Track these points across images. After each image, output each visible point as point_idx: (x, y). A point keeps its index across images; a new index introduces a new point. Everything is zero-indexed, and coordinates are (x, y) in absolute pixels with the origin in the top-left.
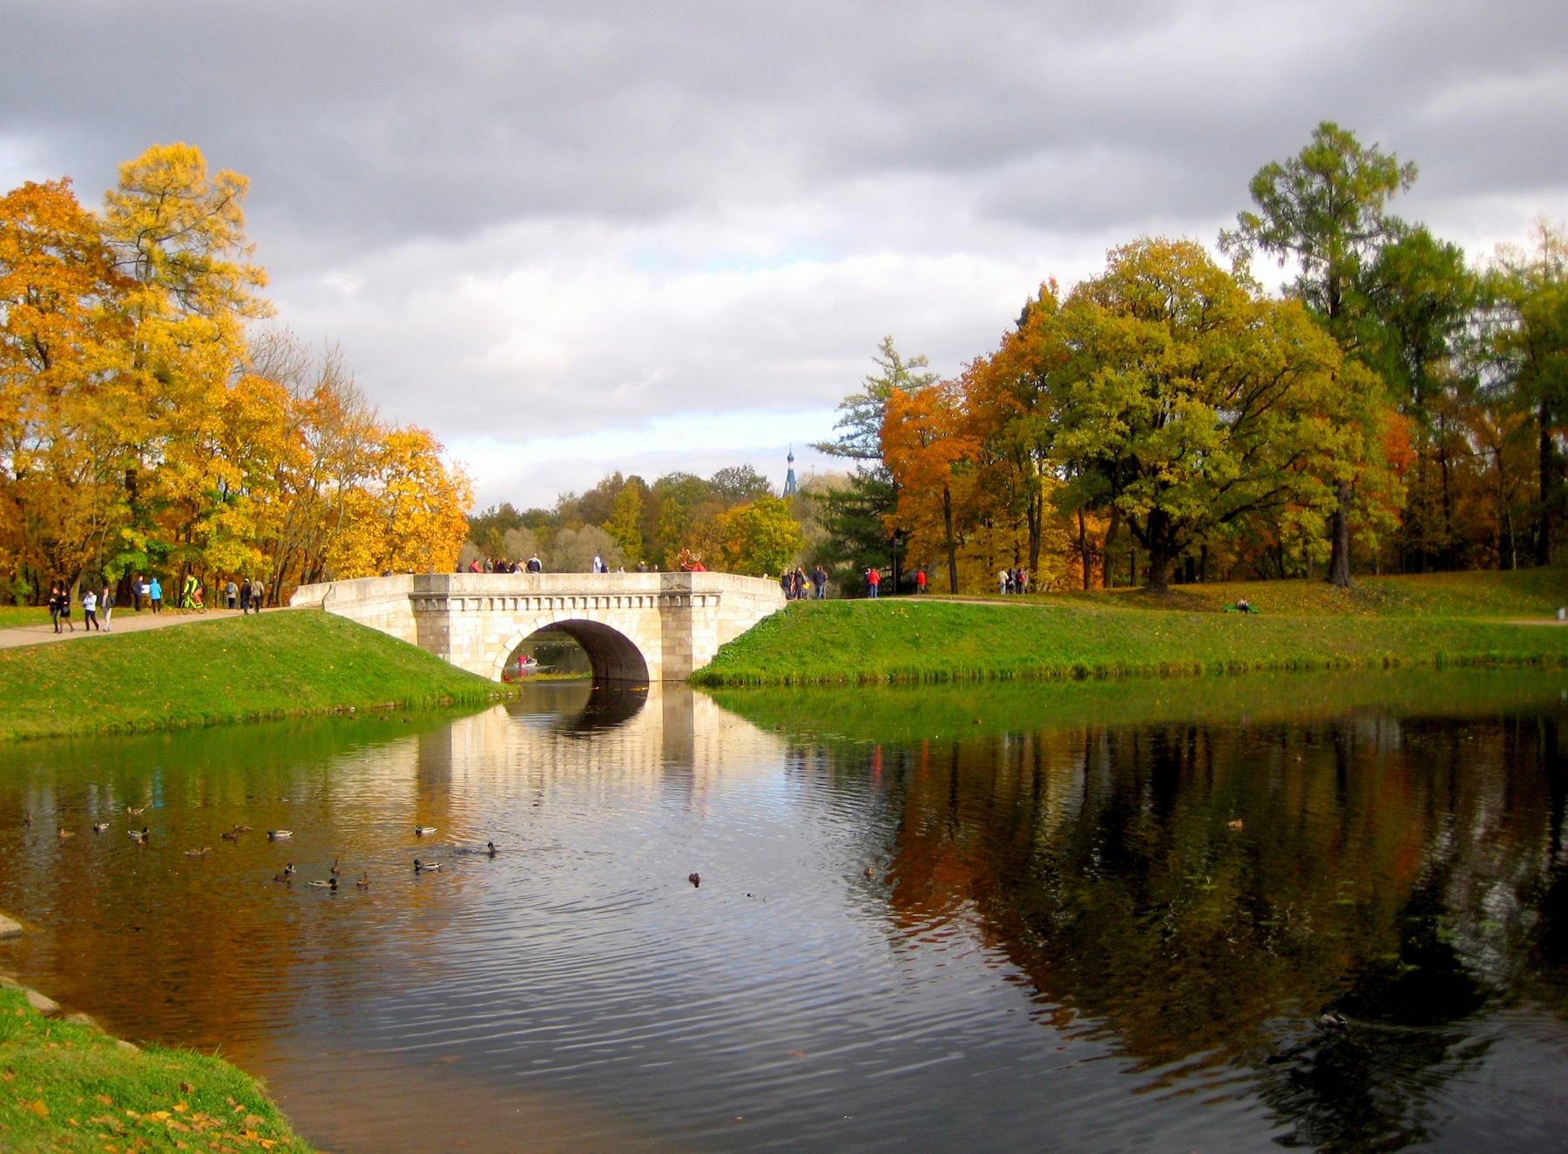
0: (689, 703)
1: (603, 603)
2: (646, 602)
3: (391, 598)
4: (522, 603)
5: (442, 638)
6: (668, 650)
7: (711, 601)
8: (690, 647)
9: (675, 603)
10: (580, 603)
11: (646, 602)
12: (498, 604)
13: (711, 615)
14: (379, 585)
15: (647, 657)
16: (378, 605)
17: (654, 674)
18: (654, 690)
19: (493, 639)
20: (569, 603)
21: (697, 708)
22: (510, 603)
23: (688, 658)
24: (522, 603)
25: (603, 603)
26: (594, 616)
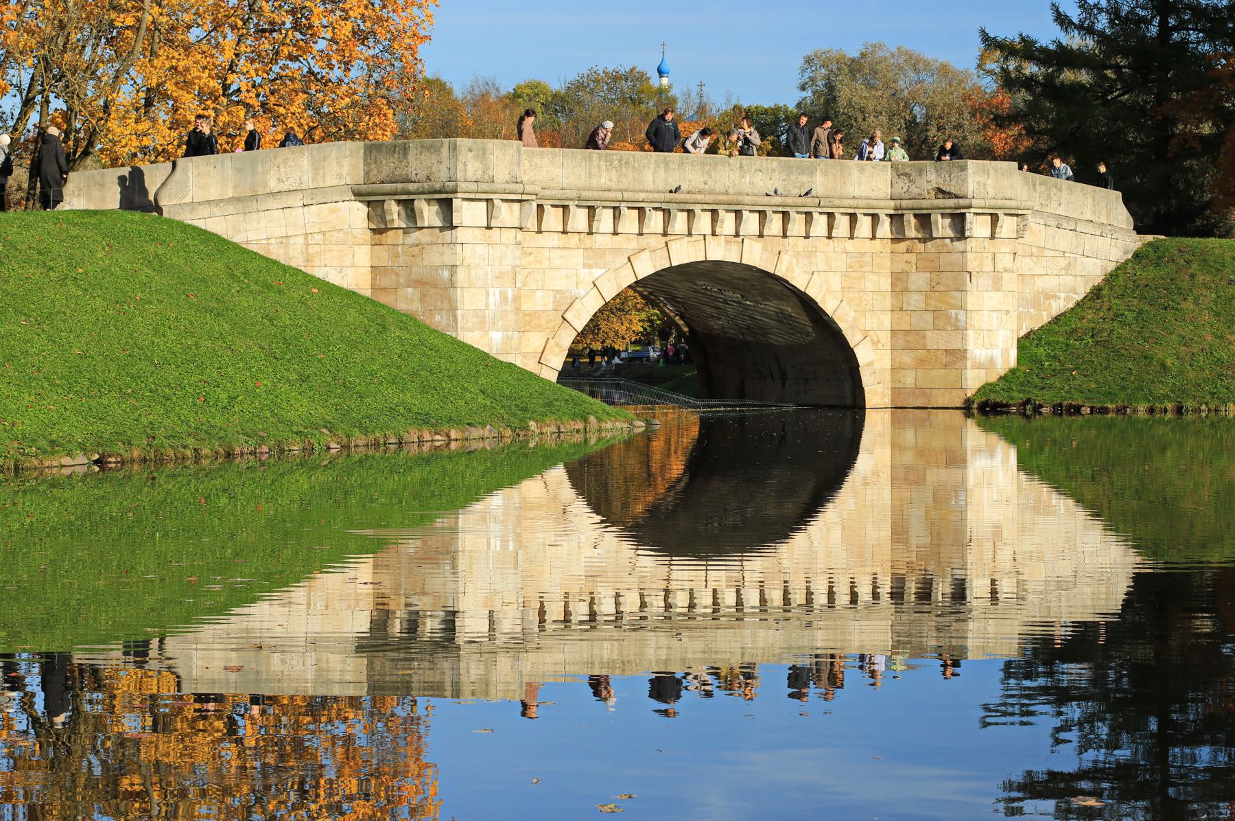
0: (957, 460)
1: (775, 224)
2: (864, 224)
3: (315, 196)
4: (605, 219)
5: (441, 288)
6: (904, 339)
7: (1007, 226)
8: (960, 329)
9: (926, 224)
10: (727, 222)
11: (864, 224)
12: (553, 218)
13: (1005, 261)
14: (296, 167)
15: (863, 354)
16: (298, 215)
17: (877, 389)
18: (876, 428)
19: (540, 302)
20: (703, 222)
21: (977, 467)
22: (579, 218)
23: (957, 356)
24: (605, 219)
25: (775, 224)
26: (756, 255)
